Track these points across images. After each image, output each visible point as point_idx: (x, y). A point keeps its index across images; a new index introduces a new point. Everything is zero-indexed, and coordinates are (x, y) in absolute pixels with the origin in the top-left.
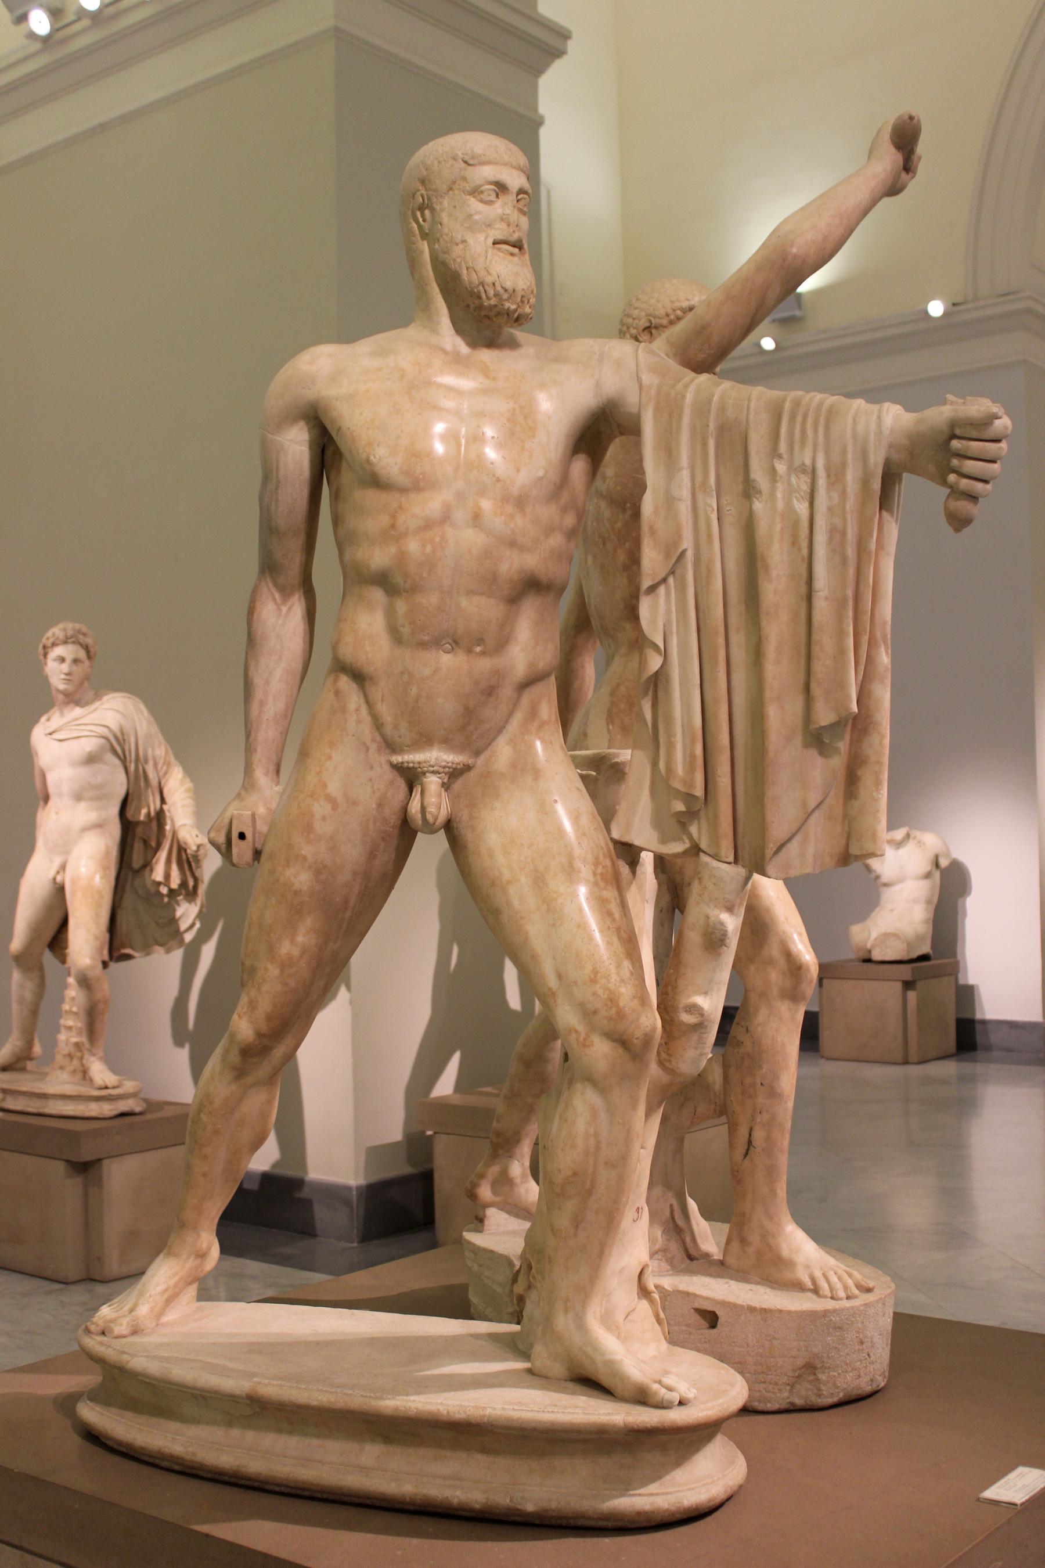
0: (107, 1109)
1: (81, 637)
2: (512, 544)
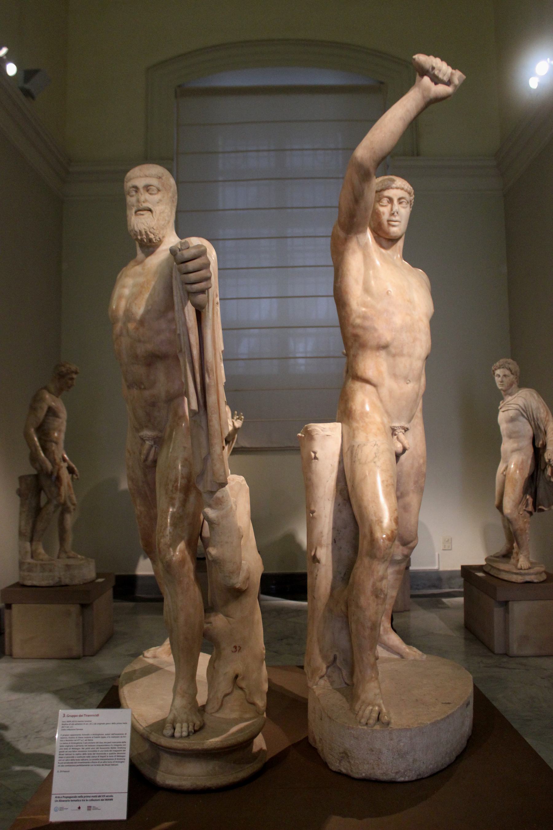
1: (507, 365)
2: (140, 341)
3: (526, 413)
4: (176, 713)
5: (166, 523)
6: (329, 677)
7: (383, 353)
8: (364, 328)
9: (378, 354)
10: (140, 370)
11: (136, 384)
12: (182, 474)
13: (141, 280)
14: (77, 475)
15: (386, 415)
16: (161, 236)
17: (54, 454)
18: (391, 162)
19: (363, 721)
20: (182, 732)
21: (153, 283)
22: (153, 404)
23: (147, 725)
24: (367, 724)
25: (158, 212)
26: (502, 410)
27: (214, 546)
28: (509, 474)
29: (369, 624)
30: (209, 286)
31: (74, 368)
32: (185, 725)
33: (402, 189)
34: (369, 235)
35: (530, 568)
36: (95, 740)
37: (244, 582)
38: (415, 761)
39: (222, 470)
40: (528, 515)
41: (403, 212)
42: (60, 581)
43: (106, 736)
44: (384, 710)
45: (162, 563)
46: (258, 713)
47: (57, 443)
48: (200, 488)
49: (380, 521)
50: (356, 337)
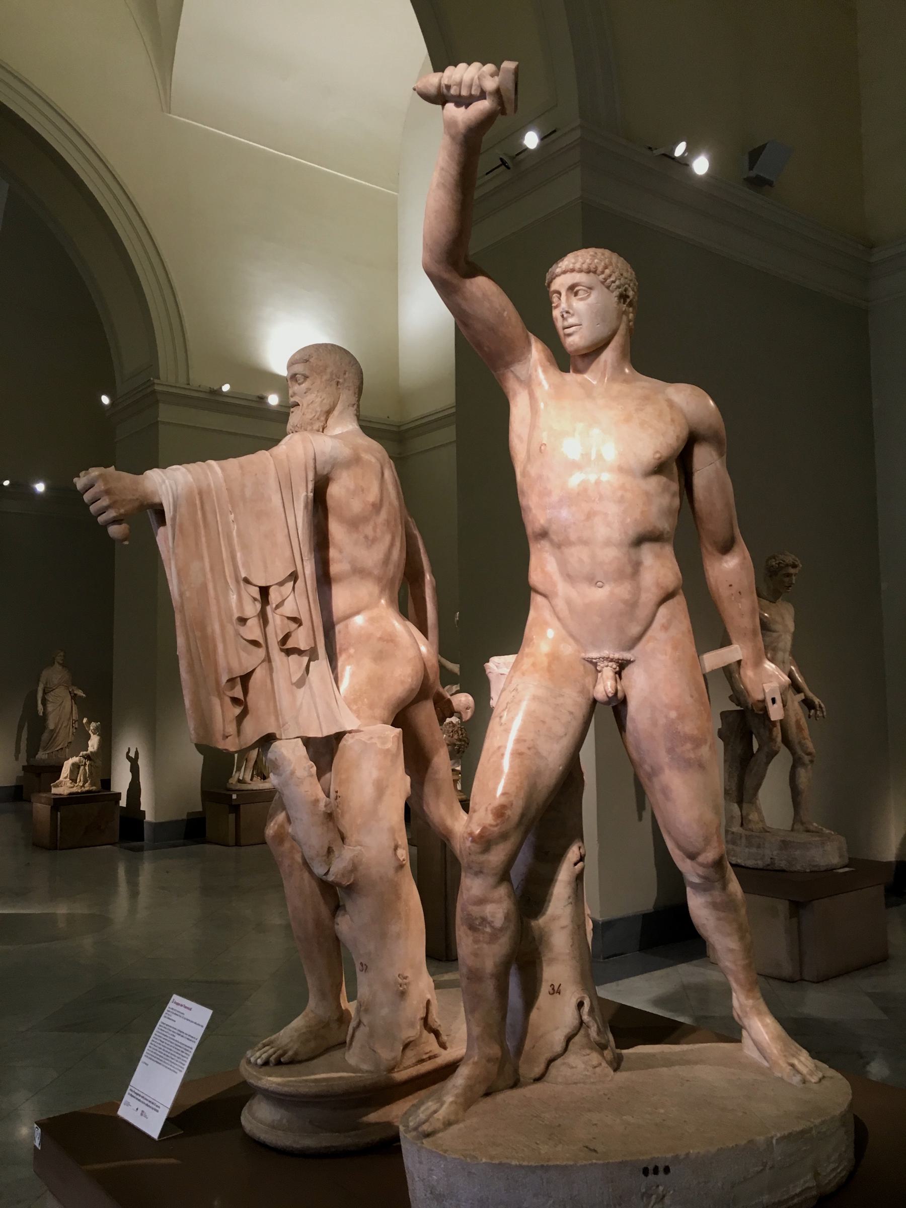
15: (571, 641)
25: (305, 405)
31: (790, 558)
36: (177, 1038)
37: (343, 875)
42: (773, 863)
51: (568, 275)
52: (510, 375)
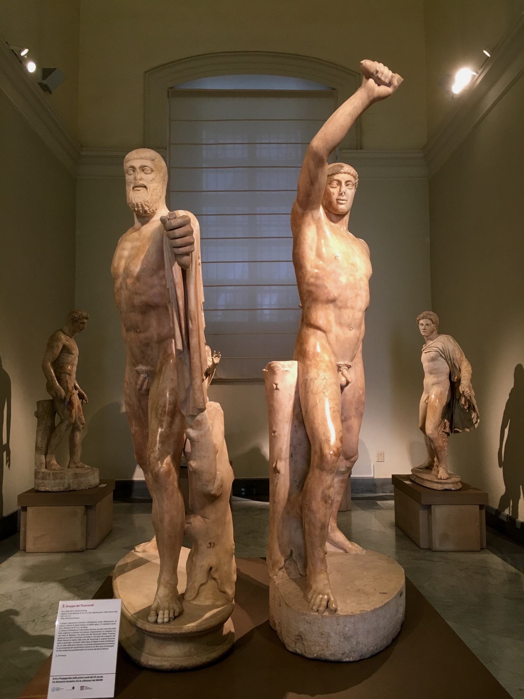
0: (439, 487)
1: (429, 316)
2: (136, 293)
3: (444, 355)
4: (159, 601)
5: (156, 441)
6: (286, 569)
7: (331, 306)
8: (317, 286)
9: (327, 306)
10: (136, 317)
11: (133, 328)
12: (169, 401)
13: (137, 244)
14: (86, 401)
15: (333, 355)
16: (154, 209)
17: (67, 384)
18: (339, 152)
19: (315, 608)
20: (164, 619)
21: (147, 247)
22: (147, 345)
23: (134, 612)
24: (318, 611)
25: (151, 189)
26: (425, 351)
27: (194, 460)
28: (430, 402)
29: (319, 525)
30: (192, 250)
31: (85, 314)
32: (166, 612)
33: (349, 174)
34: (321, 210)
35: (448, 479)
36: (89, 627)
38: (358, 643)
39: (202, 398)
40: (446, 435)
41: (350, 192)
43: (99, 623)
44: (332, 599)
45: (152, 473)
46: (228, 601)
47: (70, 375)
48: (184, 412)
49: (328, 440)
50: (310, 293)
51: (346, 175)
52: (310, 215)
